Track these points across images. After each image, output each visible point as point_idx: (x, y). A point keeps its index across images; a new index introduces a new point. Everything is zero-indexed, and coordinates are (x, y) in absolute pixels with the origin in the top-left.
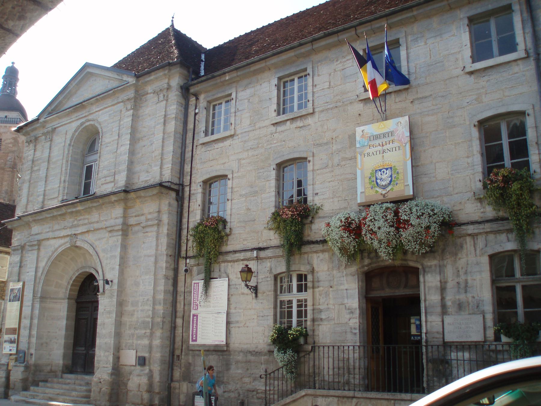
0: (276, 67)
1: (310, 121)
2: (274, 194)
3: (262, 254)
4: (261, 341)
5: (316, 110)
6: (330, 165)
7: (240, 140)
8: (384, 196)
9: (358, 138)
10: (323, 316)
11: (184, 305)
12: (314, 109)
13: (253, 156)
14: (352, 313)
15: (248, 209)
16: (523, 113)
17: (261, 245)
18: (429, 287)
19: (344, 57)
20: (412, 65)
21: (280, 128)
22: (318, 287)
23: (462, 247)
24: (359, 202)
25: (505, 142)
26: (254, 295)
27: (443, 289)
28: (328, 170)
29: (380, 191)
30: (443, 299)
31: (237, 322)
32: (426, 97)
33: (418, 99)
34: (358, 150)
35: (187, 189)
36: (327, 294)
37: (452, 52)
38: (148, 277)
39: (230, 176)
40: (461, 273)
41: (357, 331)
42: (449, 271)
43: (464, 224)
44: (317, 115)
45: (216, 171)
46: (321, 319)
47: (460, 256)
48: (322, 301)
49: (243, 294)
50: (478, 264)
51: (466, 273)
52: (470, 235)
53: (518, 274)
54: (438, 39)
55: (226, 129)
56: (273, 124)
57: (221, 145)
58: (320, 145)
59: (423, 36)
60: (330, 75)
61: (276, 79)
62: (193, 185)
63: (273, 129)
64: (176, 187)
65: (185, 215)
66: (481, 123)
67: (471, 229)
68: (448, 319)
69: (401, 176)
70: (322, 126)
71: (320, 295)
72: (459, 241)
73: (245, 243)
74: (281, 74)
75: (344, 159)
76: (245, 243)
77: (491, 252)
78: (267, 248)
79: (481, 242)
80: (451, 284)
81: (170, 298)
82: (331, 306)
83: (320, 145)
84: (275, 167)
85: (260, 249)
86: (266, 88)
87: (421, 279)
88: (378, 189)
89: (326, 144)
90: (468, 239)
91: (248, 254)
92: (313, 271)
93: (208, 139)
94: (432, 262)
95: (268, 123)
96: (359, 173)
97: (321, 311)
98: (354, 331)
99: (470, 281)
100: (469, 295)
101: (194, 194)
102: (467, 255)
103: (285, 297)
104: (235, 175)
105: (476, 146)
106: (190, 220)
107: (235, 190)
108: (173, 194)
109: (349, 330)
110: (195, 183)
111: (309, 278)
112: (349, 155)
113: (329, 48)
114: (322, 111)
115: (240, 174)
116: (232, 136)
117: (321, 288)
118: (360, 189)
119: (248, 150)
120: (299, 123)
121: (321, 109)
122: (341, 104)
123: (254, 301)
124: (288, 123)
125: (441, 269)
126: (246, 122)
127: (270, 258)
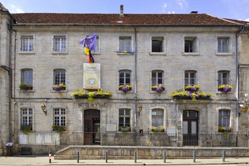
0: (54, 32)
1: (66, 56)
2: (53, 80)
3: (48, 101)
5: (69, 53)
6: (74, 74)
7: (38, 56)
8: (92, 87)
9: (84, 67)
11: (15, 116)
12: (68, 52)
14: (80, 122)
15: (42, 84)
16: (130, 71)
17: (48, 97)
18: (103, 115)
19: (79, 36)
20: (102, 47)
21: (55, 56)
22: (69, 113)
23: (112, 106)
24: (84, 88)
25: (125, 78)
26: (45, 114)
27: (106, 117)
28: (73, 75)
29: (91, 86)
30: (106, 119)
32: (105, 59)
33: (103, 59)
34: (84, 71)
35: (13, 71)
36: (72, 116)
37: (114, 46)
39: (34, 70)
40: (112, 112)
41: (82, 127)
42: (108, 112)
43: (113, 99)
44: (69, 55)
45: (27, 66)
46: (70, 123)
47: (111, 108)
48: (70, 118)
49: (41, 114)
50: (116, 111)
51: (113, 113)
52: (114, 103)
53: (125, 114)
54: (110, 40)
55: (30, 50)
56: (52, 54)
57: (28, 56)
58: (70, 66)
59: (106, 38)
60: (74, 41)
61: (53, 36)
62: (16, 70)
63: (52, 56)
64: (8, 69)
65: (13, 81)
66: (120, 71)
67: (115, 101)
68: (108, 125)
69: (97, 82)
70: (71, 59)
71: (70, 116)
72: (111, 104)
73: (41, 96)
74: (55, 35)
75: (79, 73)
76: (41, 96)
77: (119, 108)
78: (52, 99)
79: (117, 105)
80: (109, 116)
81: (8, 113)
83: (70, 66)
84: (53, 70)
85: (48, 99)
86: (49, 38)
87: (101, 113)
88: (90, 85)
89: (73, 66)
90: (114, 104)
91: (43, 100)
92: (67, 108)
93: (22, 52)
94: (104, 109)
95: (49, 53)
96: (84, 79)
97: (70, 121)
98: (81, 127)
99: (113, 116)
100: (113, 119)
101: (16, 74)
102: (113, 108)
103: (57, 116)
104: (36, 70)
105: (118, 78)
106: (15, 84)
107: (37, 75)
108: (7, 72)
109: (79, 127)
110: (17, 69)
111: (66, 110)
112: (80, 71)
113: (74, 31)
114: (71, 54)
115: (38, 70)
116: (34, 54)
117: (70, 114)
118: (84, 84)
119: (41, 61)
120: (62, 56)
121: (71, 53)
122: (78, 53)
123: (46, 116)
124: (58, 55)
125: (106, 111)
126: (40, 50)
127: (51, 102)
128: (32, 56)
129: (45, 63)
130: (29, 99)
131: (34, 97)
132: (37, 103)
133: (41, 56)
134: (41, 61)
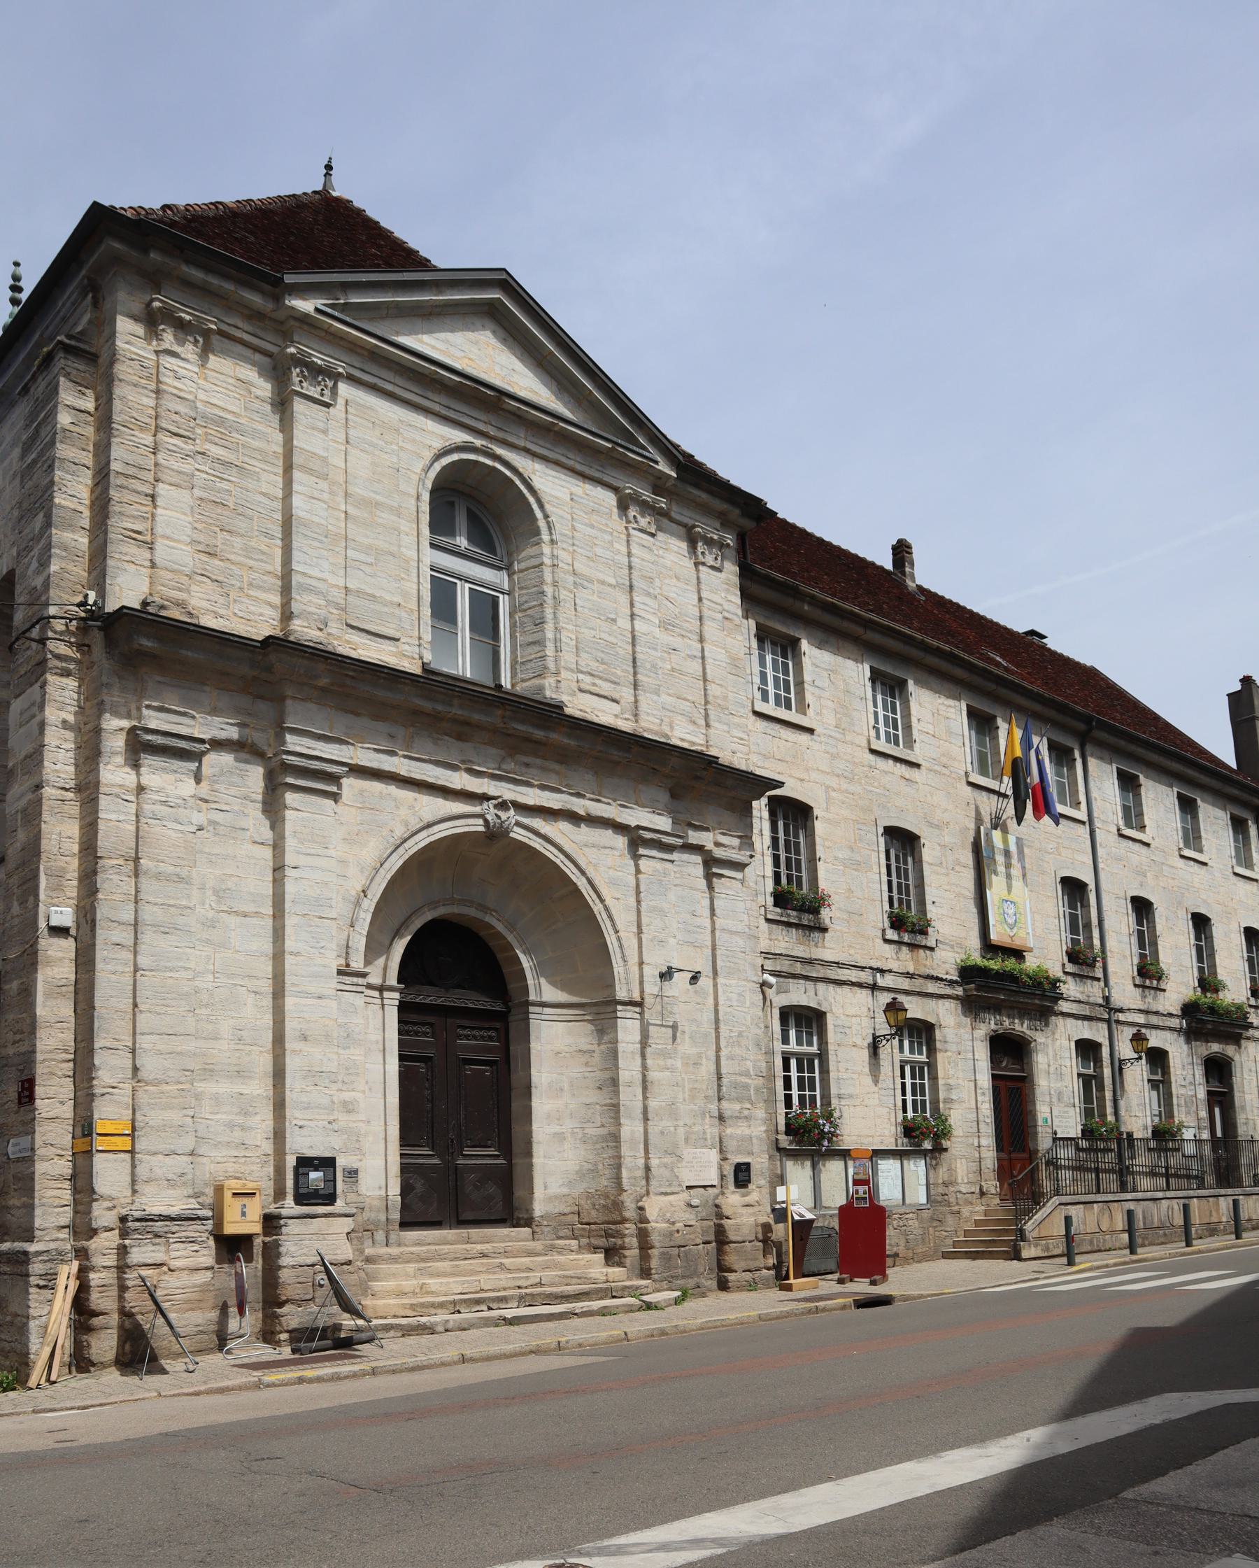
4: (887, 1132)
10: (954, 1097)
13: (846, 791)
31: (851, 1096)
38: (734, 982)
48: (951, 1072)
63: (872, 757)
73: (852, 952)
76: (852, 952)
80: (1052, 1069)
82: (960, 1082)
94: (1040, 1038)
115: (830, 816)
119: (838, 776)
120: (901, 769)
126: (830, 719)
128: (804, 738)
129: (852, 788)
130: (810, 962)
131: (828, 955)
132: (839, 990)
133: (834, 750)
134: (838, 776)
